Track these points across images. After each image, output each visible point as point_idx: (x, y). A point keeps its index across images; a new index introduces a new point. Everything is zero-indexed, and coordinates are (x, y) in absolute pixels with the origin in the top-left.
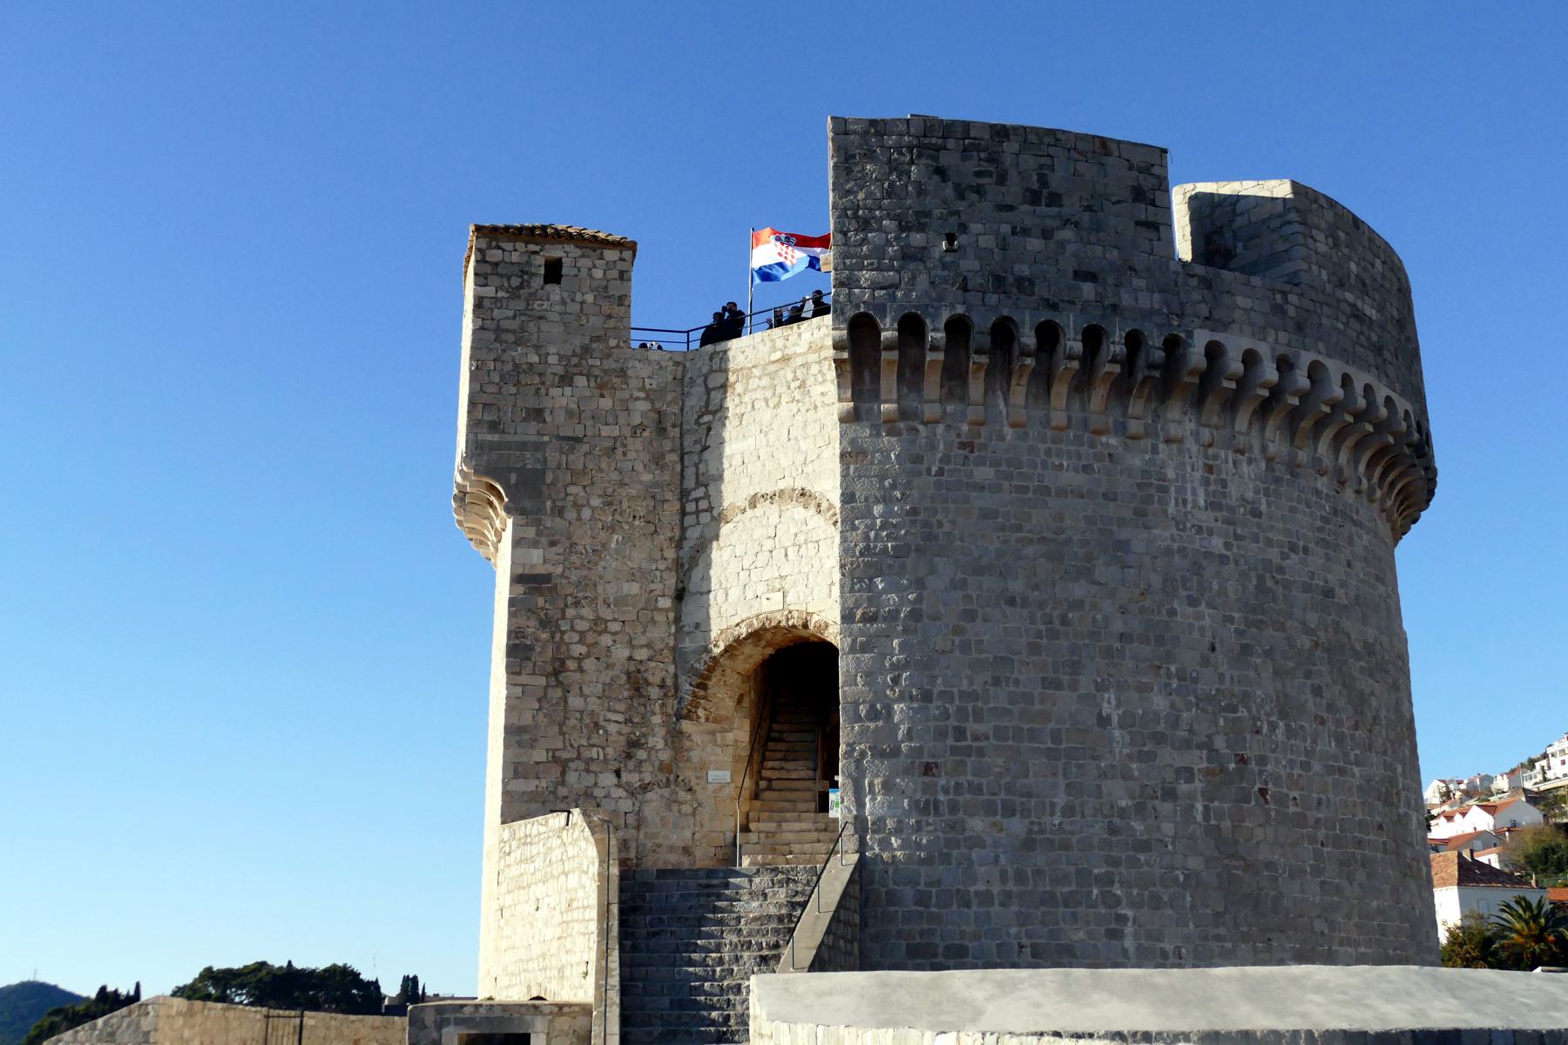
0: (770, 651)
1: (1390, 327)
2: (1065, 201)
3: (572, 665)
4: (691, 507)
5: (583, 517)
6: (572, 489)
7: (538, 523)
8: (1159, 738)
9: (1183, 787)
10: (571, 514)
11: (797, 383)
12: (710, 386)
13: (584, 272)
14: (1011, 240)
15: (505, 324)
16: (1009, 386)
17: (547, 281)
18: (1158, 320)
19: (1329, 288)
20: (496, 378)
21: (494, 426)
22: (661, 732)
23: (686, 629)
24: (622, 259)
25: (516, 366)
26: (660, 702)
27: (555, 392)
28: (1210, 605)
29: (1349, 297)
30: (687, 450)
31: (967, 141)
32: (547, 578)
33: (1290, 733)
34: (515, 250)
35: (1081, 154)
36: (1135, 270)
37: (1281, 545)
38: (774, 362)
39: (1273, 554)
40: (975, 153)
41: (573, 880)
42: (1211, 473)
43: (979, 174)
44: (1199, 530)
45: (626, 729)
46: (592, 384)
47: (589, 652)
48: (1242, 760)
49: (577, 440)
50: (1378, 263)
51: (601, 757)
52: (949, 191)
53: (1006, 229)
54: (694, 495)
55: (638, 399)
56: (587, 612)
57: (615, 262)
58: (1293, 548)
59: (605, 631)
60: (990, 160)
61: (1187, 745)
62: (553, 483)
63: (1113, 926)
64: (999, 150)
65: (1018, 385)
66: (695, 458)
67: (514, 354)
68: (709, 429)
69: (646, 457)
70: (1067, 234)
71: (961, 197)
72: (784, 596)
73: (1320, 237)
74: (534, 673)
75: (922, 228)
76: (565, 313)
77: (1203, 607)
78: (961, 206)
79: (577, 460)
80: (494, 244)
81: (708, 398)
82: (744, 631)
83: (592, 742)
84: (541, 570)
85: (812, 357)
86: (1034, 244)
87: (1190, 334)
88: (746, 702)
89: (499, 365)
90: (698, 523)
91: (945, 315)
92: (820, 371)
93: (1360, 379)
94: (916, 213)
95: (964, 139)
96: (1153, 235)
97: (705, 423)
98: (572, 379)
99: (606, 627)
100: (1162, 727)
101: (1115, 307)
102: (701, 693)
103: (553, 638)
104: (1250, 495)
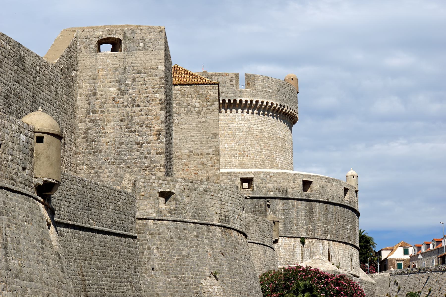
9: (236, 155)
18: (232, 97)
33: (252, 148)
37: (253, 124)
39: (252, 126)
44: (240, 123)
61: (236, 150)
77: (240, 133)
87: (237, 99)
96: (233, 86)
100: (233, 148)
101: (227, 96)
104: (248, 118)
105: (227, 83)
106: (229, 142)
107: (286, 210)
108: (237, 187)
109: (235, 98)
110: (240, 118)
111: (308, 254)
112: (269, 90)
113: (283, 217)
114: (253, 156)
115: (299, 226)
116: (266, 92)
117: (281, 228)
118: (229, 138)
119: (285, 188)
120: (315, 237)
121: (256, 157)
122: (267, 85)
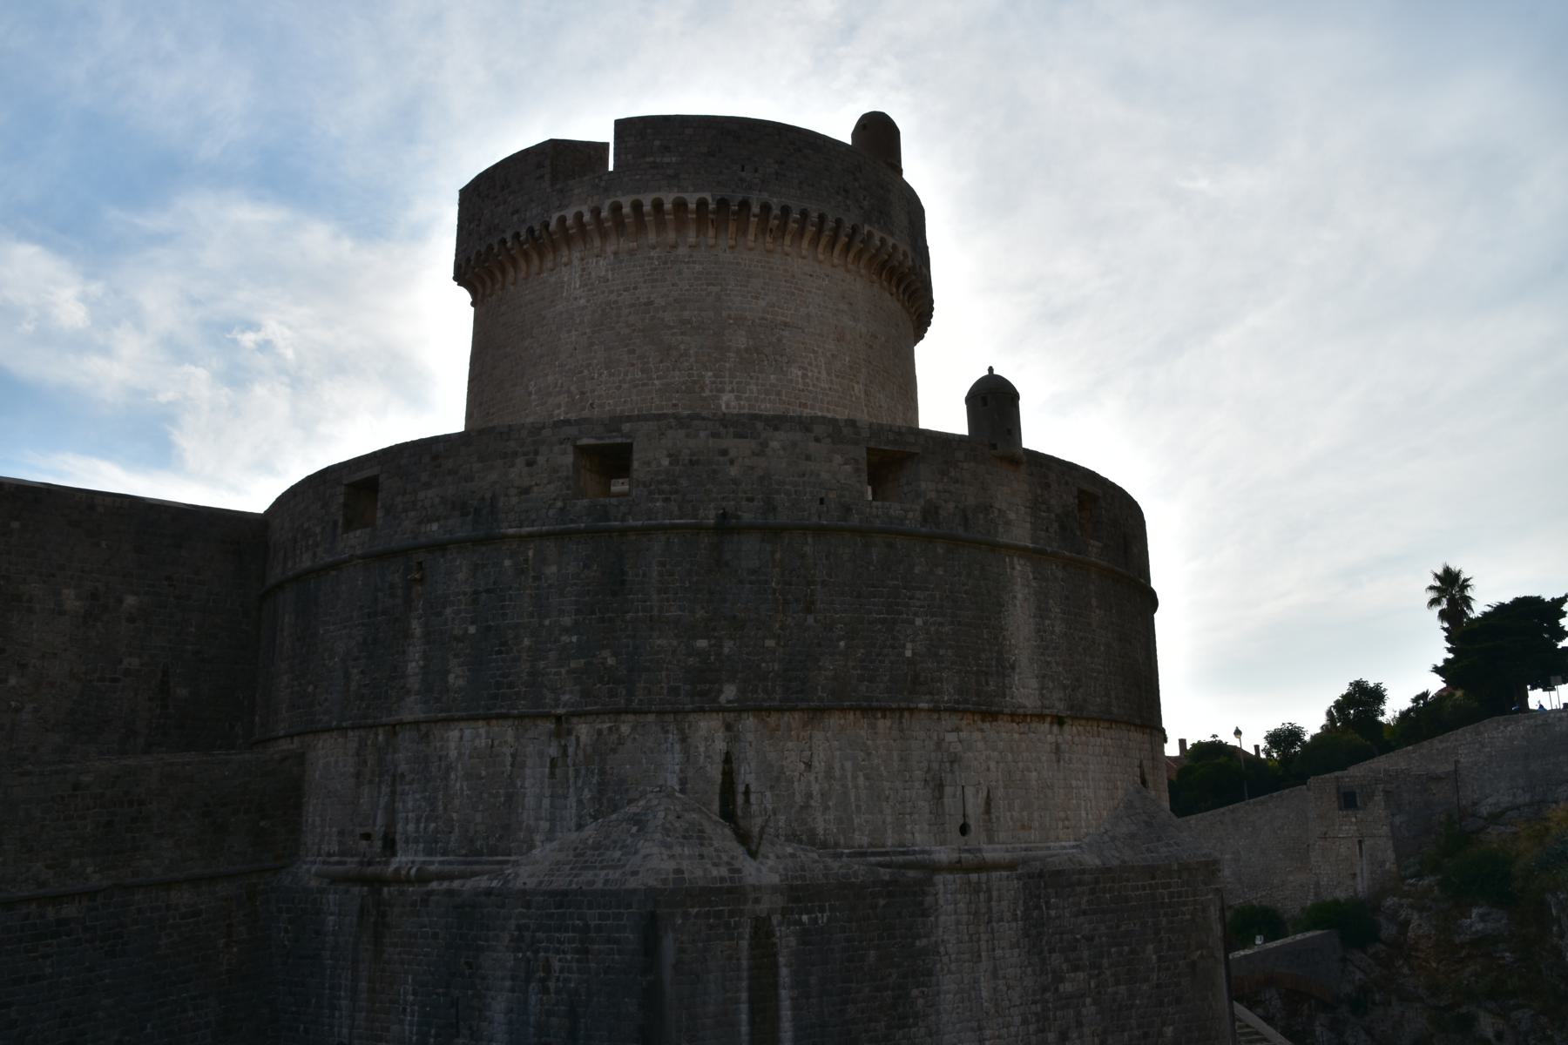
33: (611, 375)
39: (613, 297)
44: (576, 299)
48: (583, 393)
107: (484, 596)
108: (335, 523)
111: (587, 794)
112: (667, 160)
113: (472, 630)
114: (611, 402)
115: (542, 664)
117: (461, 682)
119: (488, 495)
120: (635, 705)
121: (625, 402)
122: (657, 143)
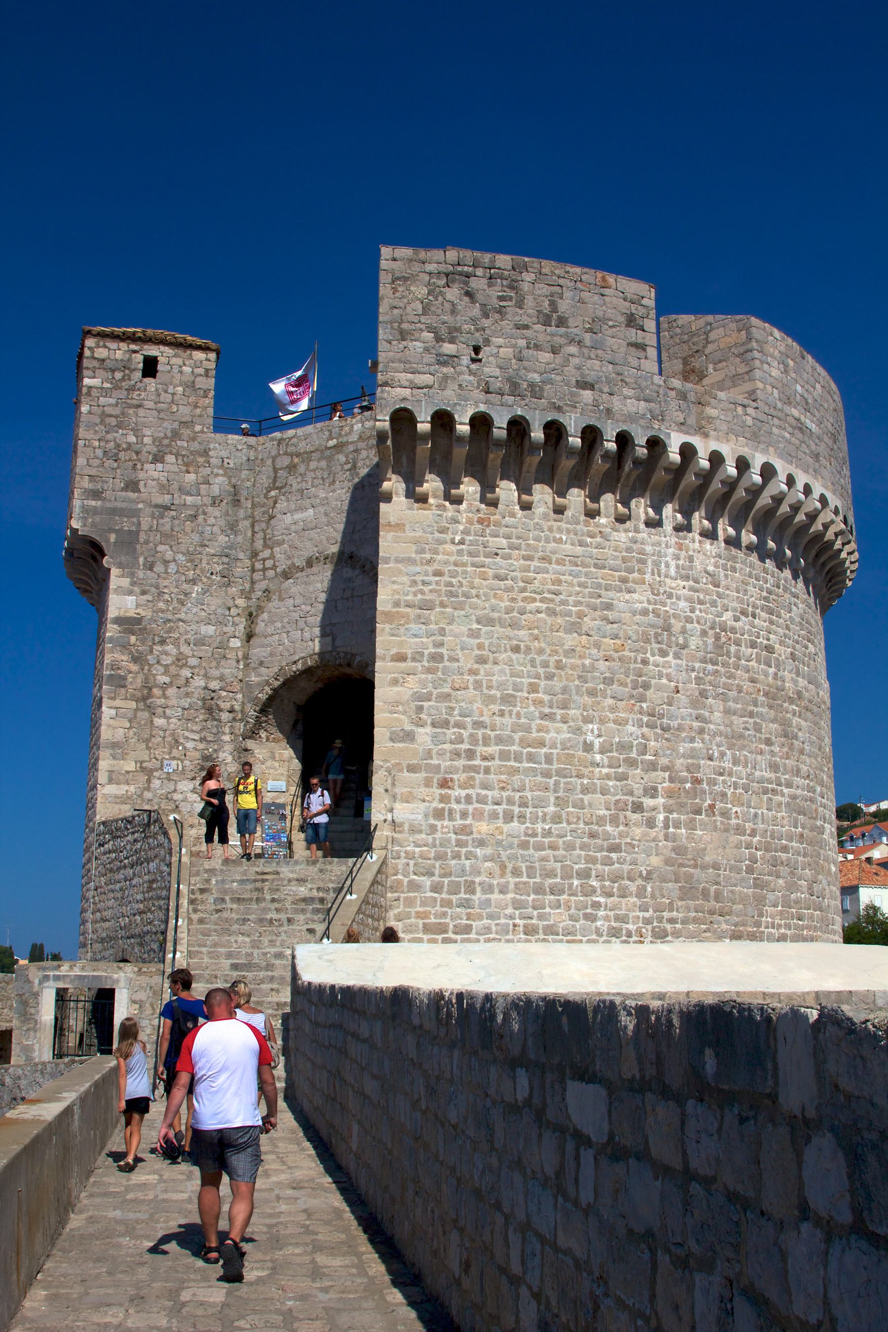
0: (320, 685)
1: (826, 439)
2: (571, 322)
3: (156, 691)
4: (258, 566)
5: (169, 571)
6: (161, 548)
7: (132, 575)
8: (632, 763)
9: (648, 802)
10: (159, 568)
11: (349, 466)
12: (277, 467)
13: (176, 370)
14: (526, 353)
15: (108, 410)
16: (521, 472)
17: (145, 375)
19: (779, 405)
20: (100, 453)
21: (96, 494)
22: (229, 748)
23: (252, 665)
24: (207, 360)
25: (118, 446)
26: (229, 724)
27: (147, 466)
28: (677, 656)
29: (795, 412)
30: (257, 518)
31: (492, 271)
32: (138, 621)
33: (736, 762)
34: (119, 349)
35: (585, 286)
36: (626, 383)
37: (734, 610)
38: (330, 448)
40: (499, 281)
41: (153, 866)
42: (681, 550)
43: (501, 298)
45: (201, 746)
46: (180, 461)
47: (171, 682)
49: (167, 508)
50: (818, 386)
51: (180, 768)
52: (476, 311)
53: (522, 343)
54: (262, 555)
55: (217, 475)
56: (170, 648)
57: (201, 362)
58: (744, 613)
59: (185, 665)
60: (512, 288)
61: (652, 767)
62: (147, 542)
63: (589, 911)
64: (519, 278)
65: (528, 472)
66: (264, 525)
67: (115, 435)
68: (275, 502)
69: (222, 523)
70: (573, 349)
71: (486, 316)
72: (334, 640)
73: (775, 364)
74: (126, 699)
75: (452, 341)
76: (160, 402)
77: (670, 658)
78: (486, 323)
79: (166, 524)
80: (101, 343)
81: (275, 477)
82: (300, 666)
83: (172, 755)
84: (131, 614)
85: (361, 445)
86: (545, 356)
88: (300, 727)
89: (103, 444)
90: (264, 579)
91: (470, 412)
92: (368, 457)
93: (801, 480)
94: (449, 328)
95: (490, 269)
96: (641, 354)
97: (272, 497)
98: (163, 457)
99: (187, 662)
100: (634, 755)
101: (608, 411)
102: (264, 719)
103: (143, 670)
104: (711, 568)
105: (610, 332)
106: (613, 709)
109: (658, 429)
110: (667, 566)
114: (738, 809)
116: (800, 429)
118: (609, 681)
121: (756, 815)
